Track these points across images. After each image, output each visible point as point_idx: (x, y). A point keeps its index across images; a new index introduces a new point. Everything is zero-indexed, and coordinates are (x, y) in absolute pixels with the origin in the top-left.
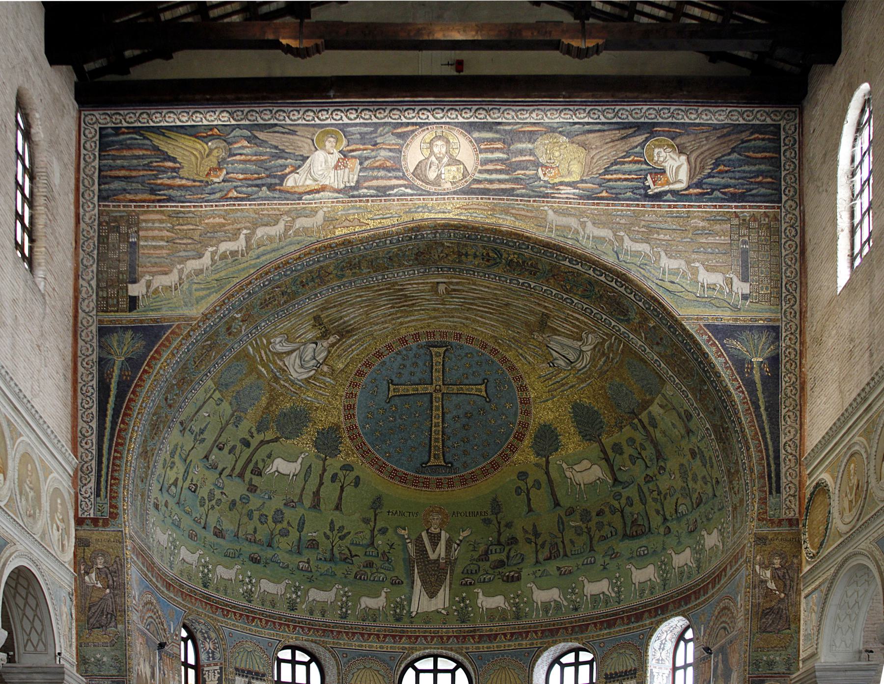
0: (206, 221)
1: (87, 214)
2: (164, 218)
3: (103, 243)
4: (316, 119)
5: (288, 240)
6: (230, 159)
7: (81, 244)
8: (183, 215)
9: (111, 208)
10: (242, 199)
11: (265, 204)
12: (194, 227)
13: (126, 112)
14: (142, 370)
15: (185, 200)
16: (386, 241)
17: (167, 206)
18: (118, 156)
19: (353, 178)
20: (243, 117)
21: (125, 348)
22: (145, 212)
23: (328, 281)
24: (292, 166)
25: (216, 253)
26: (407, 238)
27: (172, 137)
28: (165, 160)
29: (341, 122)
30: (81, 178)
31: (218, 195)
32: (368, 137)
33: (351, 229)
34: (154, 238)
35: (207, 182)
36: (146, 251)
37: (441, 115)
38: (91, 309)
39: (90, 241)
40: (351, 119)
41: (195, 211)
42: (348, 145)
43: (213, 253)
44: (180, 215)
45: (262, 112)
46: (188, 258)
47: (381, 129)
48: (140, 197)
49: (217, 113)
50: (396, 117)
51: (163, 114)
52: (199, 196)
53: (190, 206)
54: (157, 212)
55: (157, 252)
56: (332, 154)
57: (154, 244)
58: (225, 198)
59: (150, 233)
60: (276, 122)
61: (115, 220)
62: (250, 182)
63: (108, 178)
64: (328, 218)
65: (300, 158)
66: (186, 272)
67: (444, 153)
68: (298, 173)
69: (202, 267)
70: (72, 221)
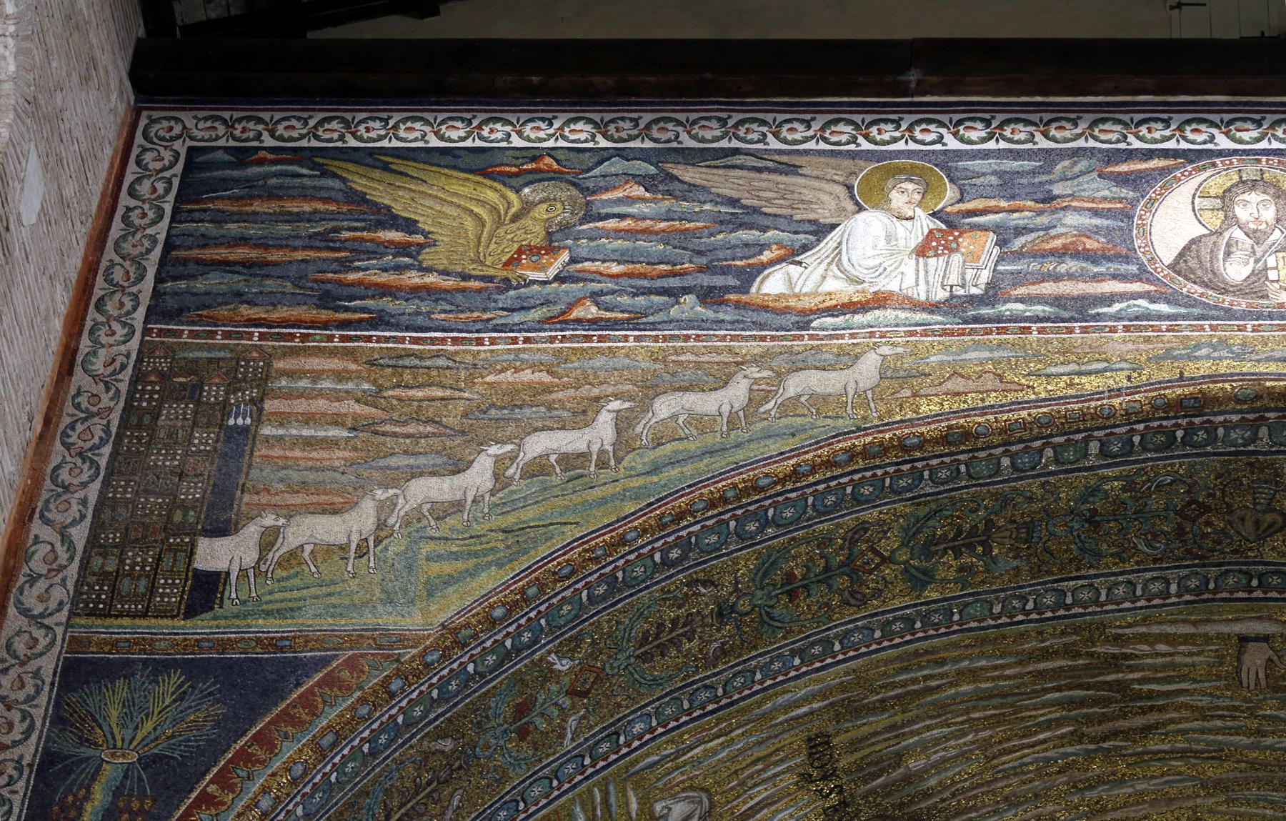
0: (490, 379)
1: (102, 352)
2: (353, 367)
3: (139, 427)
4: (861, 140)
5: (759, 426)
6: (584, 227)
7: (62, 427)
8: (417, 362)
9: (185, 338)
10: (614, 325)
11: (687, 338)
12: (448, 393)
13: (278, 116)
14: (194, 795)
15: (427, 323)
16: (1086, 440)
17: (369, 339)
18: (232, 214)
19: (976, 277)
20: (635, 132)
21: (149, 726)
22: (294, 352)
23: (877, 593)
24: (780, 245)
25: (513, 459)
26: (1160, 438)
27: (410, 173)
28: (380, 225)
29: (938, 147)
30: (104, 263)
31: (535, 315)
32: (1024, 181)
33: (972, 400)
34: (308, 419)
35: (507, 280)
36: (277, 452)
37: (1255, 134)
38: (53, 605)
39: (96, 420)
40: (971, 142)
41: (457, 353)
42: (961, 200)
43: (501, 464)
44: (407, 362)
45: (695, 122)
46: (416, 473)
47: (1066, 163)
48: (283, 312)
49: (557, 124)
50: (1109, 136)
51: (391, 123)
52: (475, 315)
53: (443, 340)
54: (333, 353)
55: (315, 454)
56: (911, 218)
57: (306, 432)
58: (560, 321)
59: (301, 406)
60: (735, 144)
61: (193, 367)
62: (645, 283)
63: (191, 266)
64: (895, 370)
65: (807, 227)
66: (403, 507)
67: (1271, 221)
68: (800, 263)
69: (459, 496)
70: (48, 364)
